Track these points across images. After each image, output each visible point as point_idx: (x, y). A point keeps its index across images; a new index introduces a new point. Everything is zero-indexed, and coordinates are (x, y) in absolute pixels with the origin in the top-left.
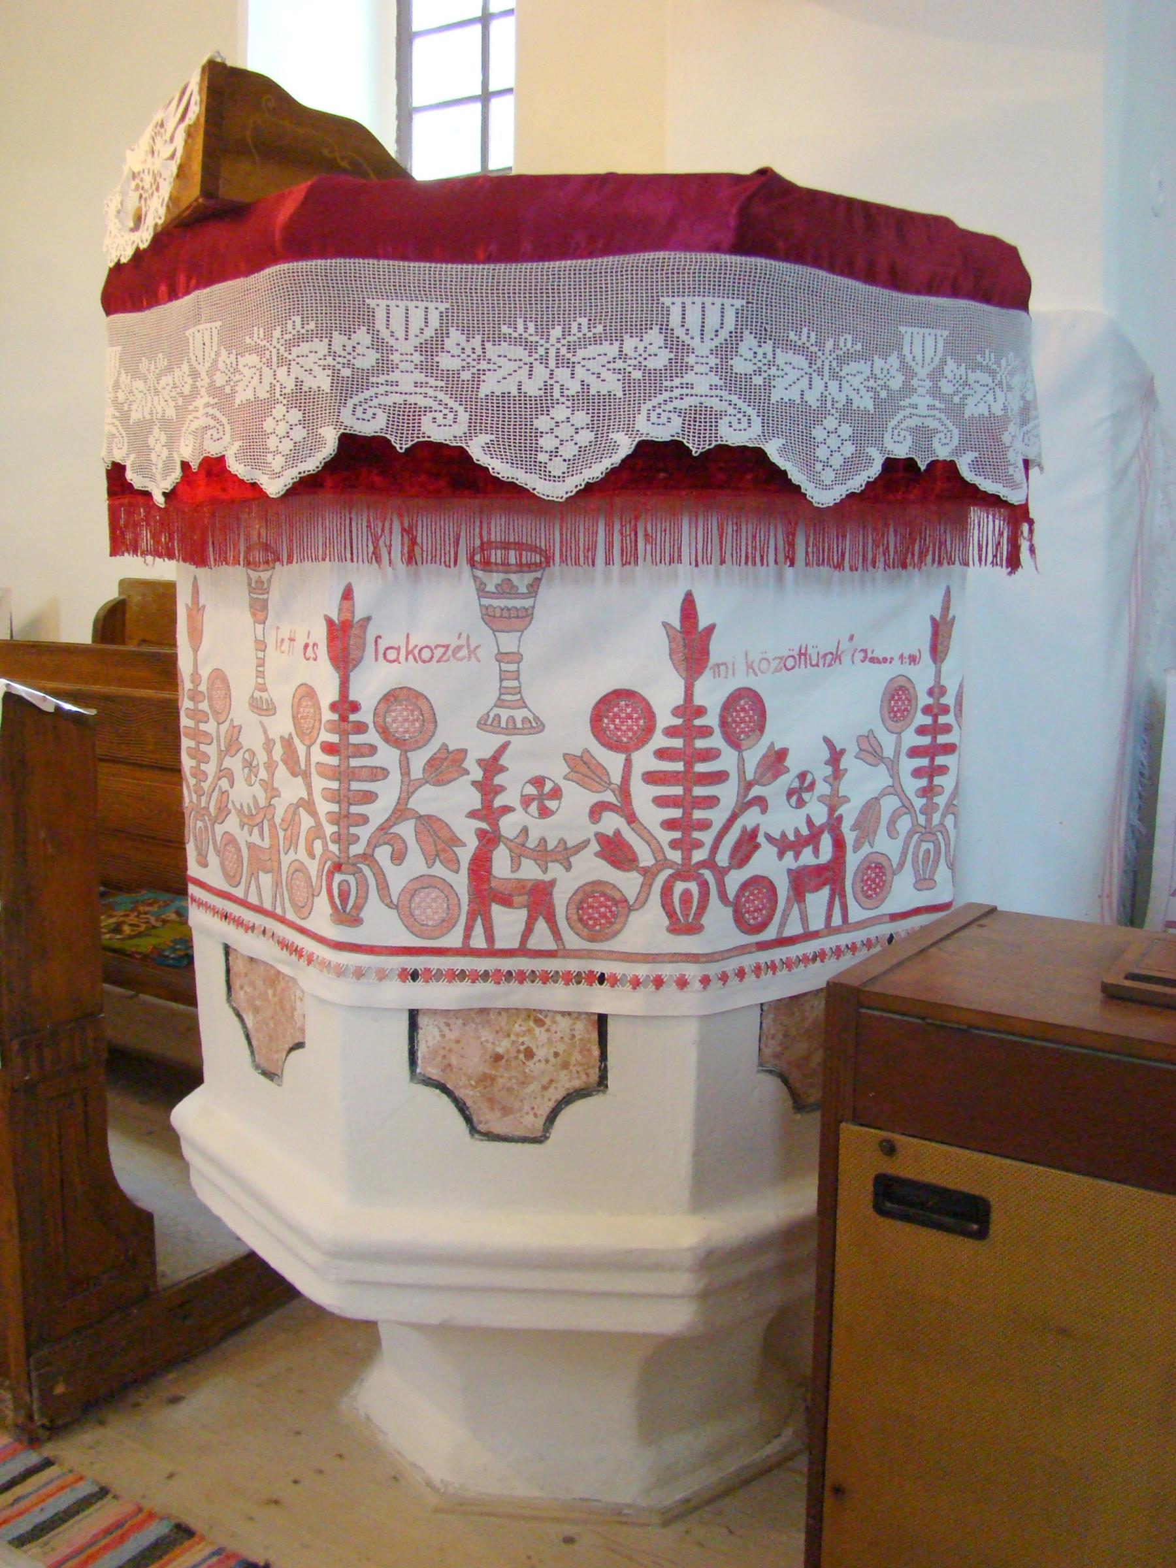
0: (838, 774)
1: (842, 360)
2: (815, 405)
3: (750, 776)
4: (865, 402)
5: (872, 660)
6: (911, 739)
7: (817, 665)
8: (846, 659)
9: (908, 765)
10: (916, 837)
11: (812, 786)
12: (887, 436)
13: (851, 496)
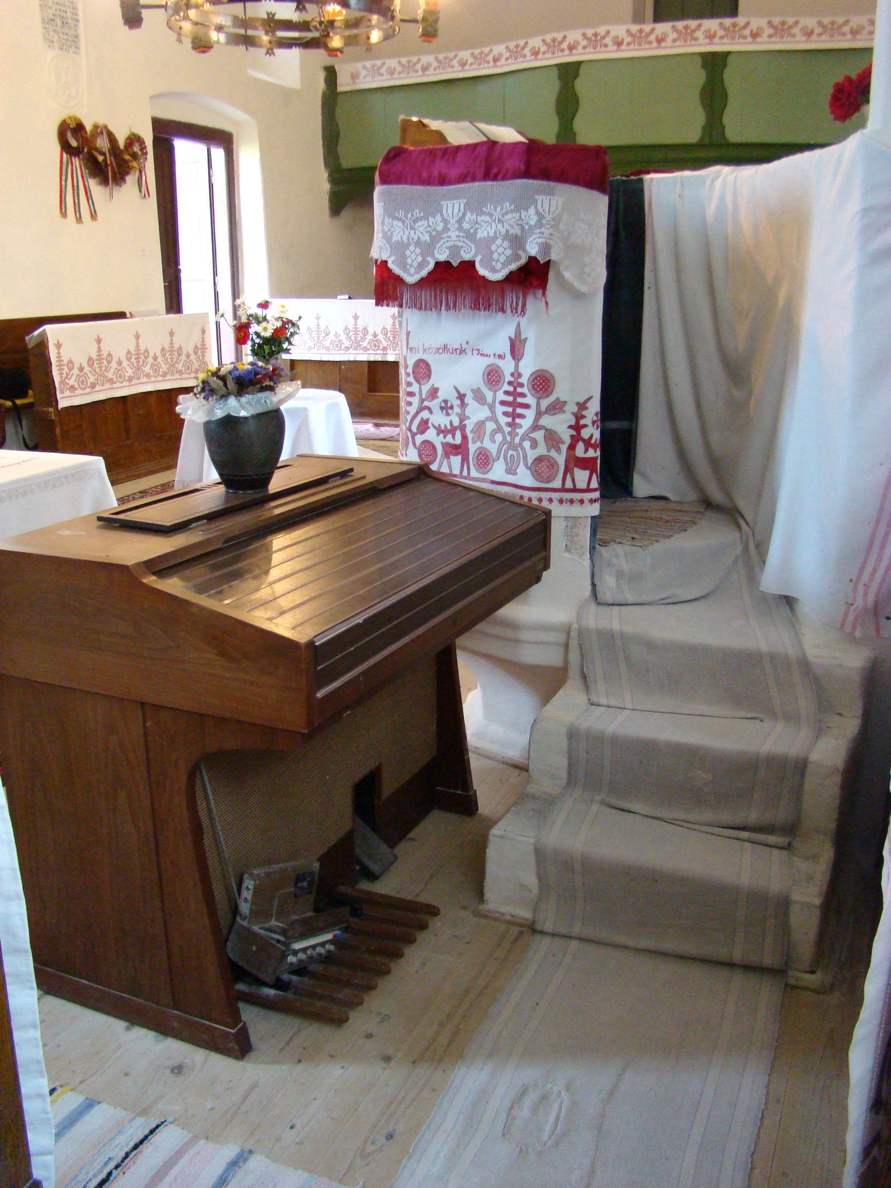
0: (463, 405)
1: (415, 221)
2: (406, 241)
3: (424, 397)
4: (426, 238)
5: (482, 355)
6: (501, 396)
7: (453, 353)
8: (469, 352)
9: (499, 409)
10: (505, 446)
11: (452, 407)
12: (436, 252)
13: (422, 279)
